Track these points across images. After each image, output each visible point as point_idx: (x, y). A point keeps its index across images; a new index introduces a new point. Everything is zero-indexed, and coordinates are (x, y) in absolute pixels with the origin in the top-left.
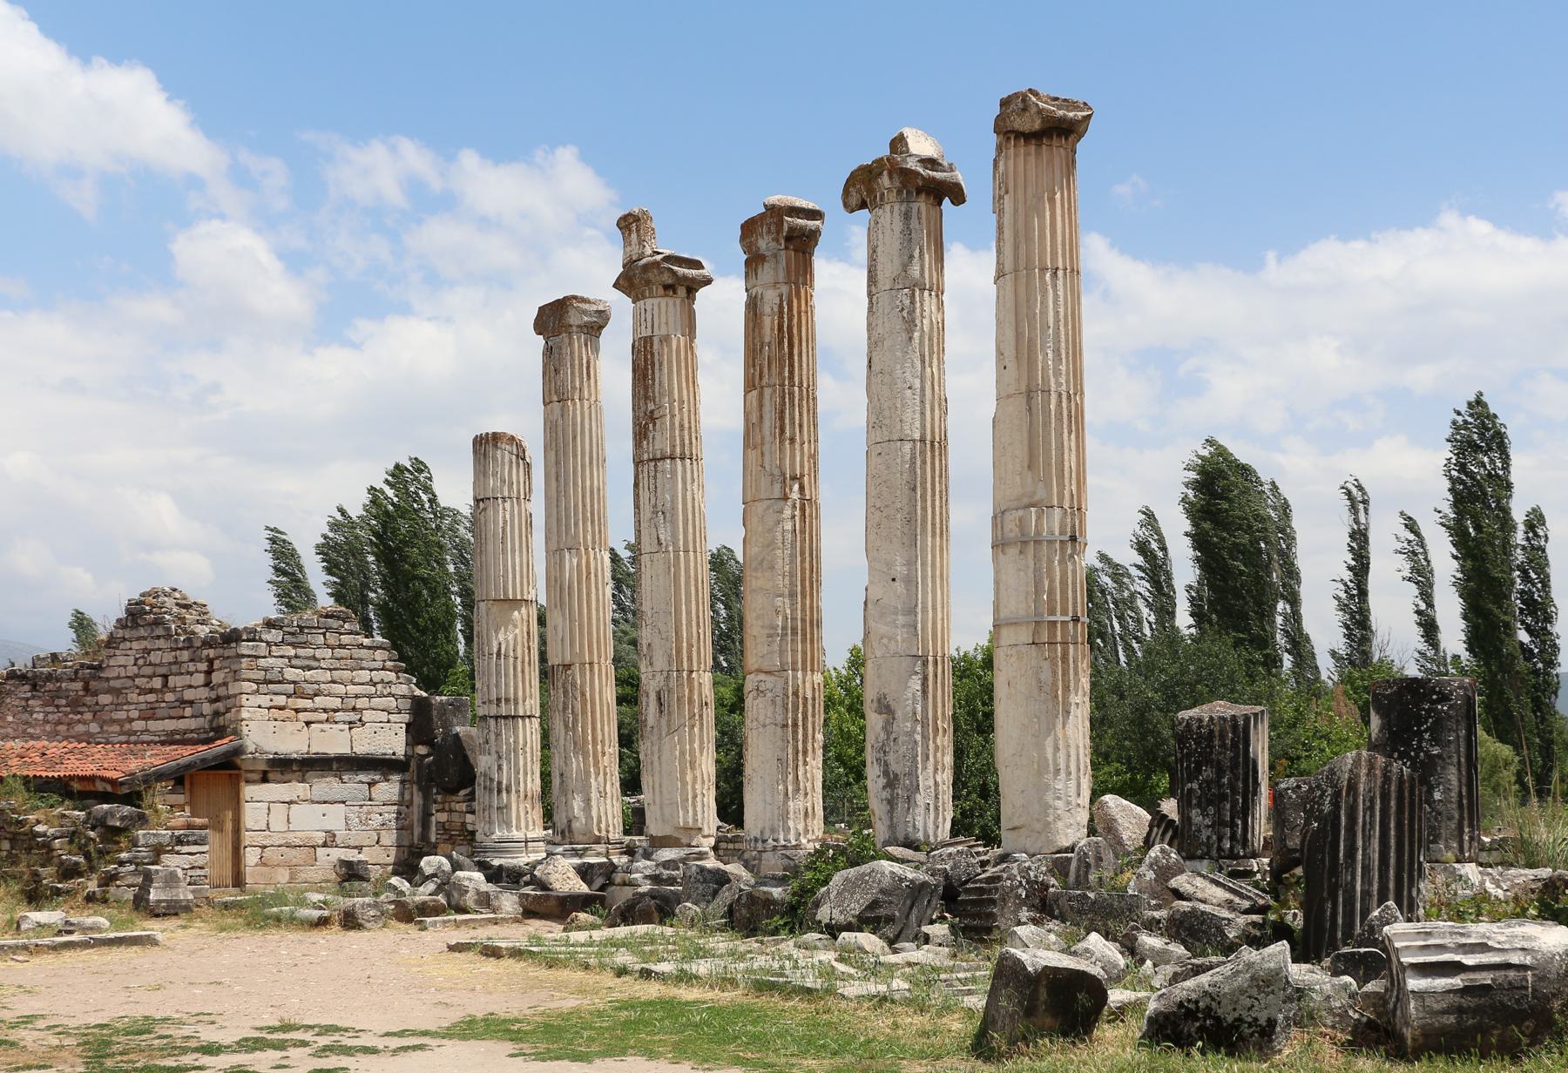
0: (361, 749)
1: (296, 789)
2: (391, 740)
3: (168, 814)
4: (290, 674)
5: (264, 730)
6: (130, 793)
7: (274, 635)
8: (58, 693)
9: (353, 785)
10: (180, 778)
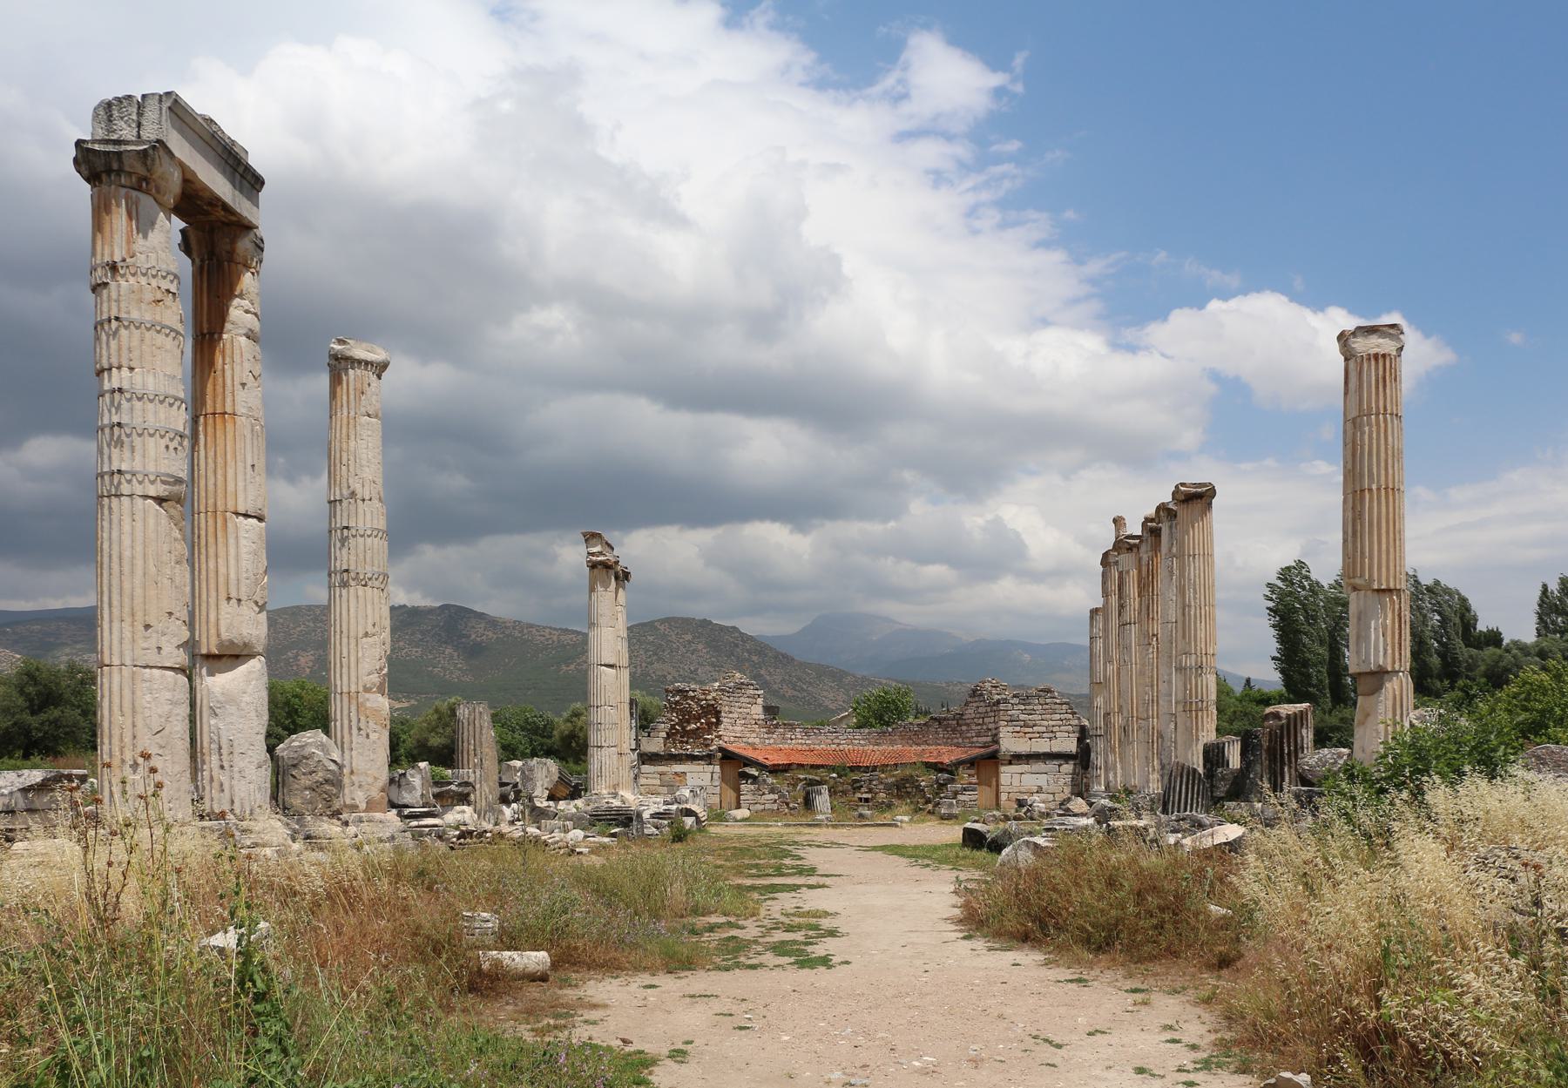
0: (1055, 750)
1: (1025, 768)
2: (1071, 746)
3: (965, 776)
4: (1022, 717)
5: (1010, 742)
6: (951, 770)
7: (1016, 700)
8: (948, 726)
9: (1051, 766)
10: (972, 763)
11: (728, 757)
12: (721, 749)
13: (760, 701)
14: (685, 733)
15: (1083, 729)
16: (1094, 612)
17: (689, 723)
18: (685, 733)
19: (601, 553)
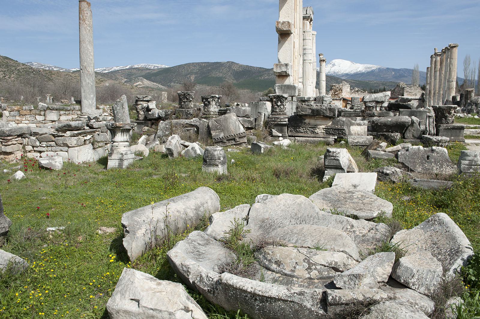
0: (416, 98)
4: (409, 91)
7: (408, 87)
11: (344, 100)
12: (343, 98)
13: (349, 88)
14: (335, 95)
15: (423, 94)
16: (428, 68)
17: (336, 92)
18: (335, 95)
19: (322, 58)
